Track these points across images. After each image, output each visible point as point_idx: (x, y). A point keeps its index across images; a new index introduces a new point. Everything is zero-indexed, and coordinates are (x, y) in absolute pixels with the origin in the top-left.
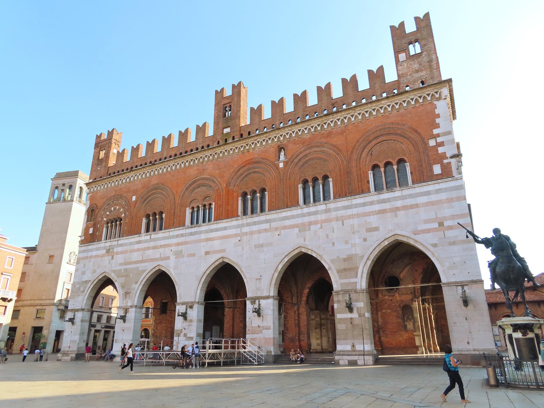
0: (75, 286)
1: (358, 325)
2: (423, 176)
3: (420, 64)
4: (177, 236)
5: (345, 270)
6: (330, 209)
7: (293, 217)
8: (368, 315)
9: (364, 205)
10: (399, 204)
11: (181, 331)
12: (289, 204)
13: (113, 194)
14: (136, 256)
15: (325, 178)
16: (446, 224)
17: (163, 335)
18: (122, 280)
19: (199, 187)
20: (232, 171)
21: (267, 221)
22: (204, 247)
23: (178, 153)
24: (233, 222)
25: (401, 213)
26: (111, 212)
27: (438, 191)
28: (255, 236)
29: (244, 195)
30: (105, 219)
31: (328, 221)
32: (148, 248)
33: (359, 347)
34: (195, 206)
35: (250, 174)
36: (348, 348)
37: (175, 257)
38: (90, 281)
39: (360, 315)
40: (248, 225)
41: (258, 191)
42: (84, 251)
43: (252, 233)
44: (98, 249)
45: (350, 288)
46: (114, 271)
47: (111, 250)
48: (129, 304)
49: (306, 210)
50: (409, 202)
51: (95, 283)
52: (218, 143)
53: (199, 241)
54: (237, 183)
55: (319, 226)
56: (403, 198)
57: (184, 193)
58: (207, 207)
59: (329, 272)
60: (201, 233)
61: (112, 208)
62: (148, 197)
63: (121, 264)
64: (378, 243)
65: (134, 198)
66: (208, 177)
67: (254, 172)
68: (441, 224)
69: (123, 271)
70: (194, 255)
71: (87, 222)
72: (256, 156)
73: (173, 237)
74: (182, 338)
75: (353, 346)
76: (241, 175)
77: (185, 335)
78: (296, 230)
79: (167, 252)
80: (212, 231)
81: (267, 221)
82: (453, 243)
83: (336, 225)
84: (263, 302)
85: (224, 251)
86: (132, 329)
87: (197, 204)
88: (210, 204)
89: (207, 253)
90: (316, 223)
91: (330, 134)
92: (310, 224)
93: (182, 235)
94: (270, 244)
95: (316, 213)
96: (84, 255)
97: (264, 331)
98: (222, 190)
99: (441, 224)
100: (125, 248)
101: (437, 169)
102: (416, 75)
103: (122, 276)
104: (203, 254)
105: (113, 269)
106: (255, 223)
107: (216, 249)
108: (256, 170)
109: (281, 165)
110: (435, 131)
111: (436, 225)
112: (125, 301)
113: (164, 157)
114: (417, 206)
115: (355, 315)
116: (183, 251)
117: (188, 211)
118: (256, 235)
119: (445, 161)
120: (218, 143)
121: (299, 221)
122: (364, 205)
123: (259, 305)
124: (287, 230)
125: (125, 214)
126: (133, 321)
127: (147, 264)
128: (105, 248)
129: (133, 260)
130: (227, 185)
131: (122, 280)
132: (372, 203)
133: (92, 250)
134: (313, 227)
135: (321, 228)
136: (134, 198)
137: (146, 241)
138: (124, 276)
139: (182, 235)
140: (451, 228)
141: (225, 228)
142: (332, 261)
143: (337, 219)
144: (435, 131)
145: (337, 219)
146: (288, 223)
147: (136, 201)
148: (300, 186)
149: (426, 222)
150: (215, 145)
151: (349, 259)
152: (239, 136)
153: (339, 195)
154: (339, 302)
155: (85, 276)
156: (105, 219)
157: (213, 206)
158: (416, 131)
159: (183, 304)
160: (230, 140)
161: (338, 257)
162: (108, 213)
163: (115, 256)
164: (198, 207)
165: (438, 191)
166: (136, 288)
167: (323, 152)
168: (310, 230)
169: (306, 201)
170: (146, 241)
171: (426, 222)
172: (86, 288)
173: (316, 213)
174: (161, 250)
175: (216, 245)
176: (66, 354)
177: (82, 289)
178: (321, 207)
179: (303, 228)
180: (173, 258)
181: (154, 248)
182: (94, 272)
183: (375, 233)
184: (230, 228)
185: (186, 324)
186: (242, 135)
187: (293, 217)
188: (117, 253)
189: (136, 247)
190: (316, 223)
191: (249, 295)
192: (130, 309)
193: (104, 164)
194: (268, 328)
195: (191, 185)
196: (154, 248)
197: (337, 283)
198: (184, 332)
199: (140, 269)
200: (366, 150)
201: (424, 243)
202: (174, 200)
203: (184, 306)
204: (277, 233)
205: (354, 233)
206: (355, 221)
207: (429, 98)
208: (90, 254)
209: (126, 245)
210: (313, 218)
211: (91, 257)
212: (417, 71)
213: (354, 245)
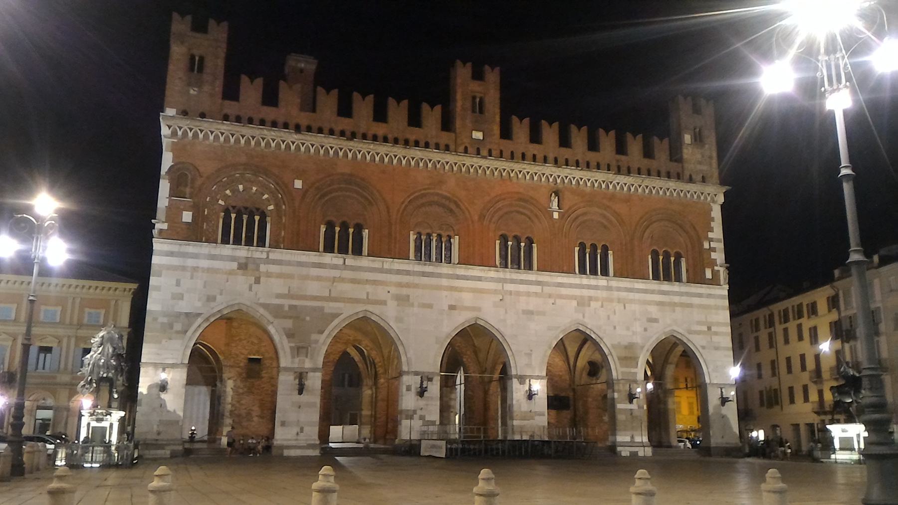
0: (155, 319)
1: (636, 417)
2: (697, 278)
3: (703, 156)
4: (399, 272)
5: (626, 358)
6: (611, 287)
7: (571, 286)
8: (645, 407)
9: (645, 291)
10: (676, 299)
11: (415, 412)
12: (565, 268)
13: (243, 159)
14: (313, 288)
15: (605, 249)
16: (714, 329)
17: (254, 414)
18: (289, 324)
19: (430, 204)
20: (487, 198)
21: (538, 283)
22: (445, 299)
23: (390, 136)
24: (492, 273)
25: (678, 309)
26: (235, 191)
27: (709, 296)
28: (523, 299)
29: (504, 239)
30: (220, 202)
31: (611, 300)
32: (342, 280)
33: (638, 439)
34: (424, 231)
35: (512, 212)
36: (628, 439)
37: (396, 303)
38: (199, 315)
39: (639, 407)
40: (513, 281)
41: (523, 239)
42: (171, 254)
43: (518, 294)
44: (213, 257)
45: (630, 378)
46: (265, 306)
47: (250, 266)
48: (308, 364)
49: (586, 280)
50: (685, 299)
51: (212, 320)
52: (466, 148)
53: (439, 288)
54: (494, 220)
55: (600, 303)
56: (681, 294)
57: (406, 206)
58: (444, 239)
59: (609, 358)
60: (440, 276)
61: (241, 187)
62: (331, 192)
63: (279, 296)
64: (657, 335)
65: (298, 184)
66: (449, 195)
67: (518, 212)
68: (709, 328)
69: (286, 308)
70: (430, 306)
71: (171, 195)
72: (521, 190)
73: (389, 271)
74: (417, 423)
75: (632, 437)
76: (500, 209)
77: (422, 418)
78: (574, 303)
79: (381, 293)
80: (458, 277)
81: (538, 283)
82: (717, 348)
83: (619, 307)
84: (533, 382)
85: (479, 309)
86: (319, 406)
87: (429, 231)
88: (450, 237)
89: (452, 308)
90: (597, 299)
91: (612, 197)
92: (590, 299)
93: (408, 273)
94: (543, 313)
95: (596, 288)
96: (175, 261)
97: (537, 418)
98: (473, 222)
99: (709, 328)
100: (286, 269)
101: (709, 274)
102: (699, 167)
103: (285, 317)
104: (446, 308)
105: (261, 301)
106: (522, 282)
107: (468, 303)
108: (521, 210)
109: (556, 215)
110: (710, 235)
111: (705, 328)
112: (297, 360)
113: (362, 131)
114: (690, 306)
115: (634, 406)
116: (411, 298)
117: (413, 237)
118: (524, 298)
119: (716, 268)
120: (466, 148)
121: (577, 292)
122: (645, 291)
123: (530, 385)
124: (564, 301)
125: (276, 205)
126: (318, 392)
127: (341, 305)
128: (233, 259)
129: (308, 294)
130: (480, 218)
131: (289, 324)
132: (652, 292)
133: (196, 256)
134: (592, 303)
135: (602, 306)
136: (298, 184)
137: (335, 267)
138: (290, 317)
139: (408, 273)
140: (716, 333)
141: (479, 279)
142: (613, 346)
143: (619, 300)
144: (710, 235)
145: (619, 300)
146: (564, 291)
147: (304, 192)
148: (577, 249)
149: (699, 323)
150: (461, 149)
151: (630, 347)
152: (498, 152)
153: (619, 274)
154: (619, 391)
155: (180, 302)
156: (220, 202)
157: (455, 241)
158: (694, 228)
159: (416, 373)
160: (484, 152)
161: (619, 343)
162: (228, 192)
163: (262, 279)
164: (429, 235)
165: (709, 296)
166: (321, 341)
167: (604, 217)
168: (589, 306)
169: (582, 271)
170: (335, 267)
171: (699, 323)
172: (190, 325)
173: (596, 288)
174: (369, 288)
175: (467, 299)
176: (156, 445)
177: (178, 327)
178: (602, 281)
179: (583, 303)
180: (392, 304)
181: (354, 281)
182: (211, 299)
183: (655, 324)
184: (487, 279)
185: (422, 402)
186: (501, 152)
187: (571, 286)
188: (269, 275)
189: (315, 272)
190: (597, 299)
191: (514, 372)
192: (311, 374)
193: (206, 88)
194: (542, 414)
195: (417, 198)
196: (354, 281)
197: (617, 370)
198: (419, 413)
199: (327, 311)
200: (648, 231)
201: (696, 343)
202: (388, 212)
203: (419, 378)
204: (552, 301)
205: (635, 319)
206: (636, 307)
207: (709, 199)
208: (190, 262)
209: (289, 263)
210: (592, 293)
211: (195, 269)
212: (700, 163)
213: (634, 333)
